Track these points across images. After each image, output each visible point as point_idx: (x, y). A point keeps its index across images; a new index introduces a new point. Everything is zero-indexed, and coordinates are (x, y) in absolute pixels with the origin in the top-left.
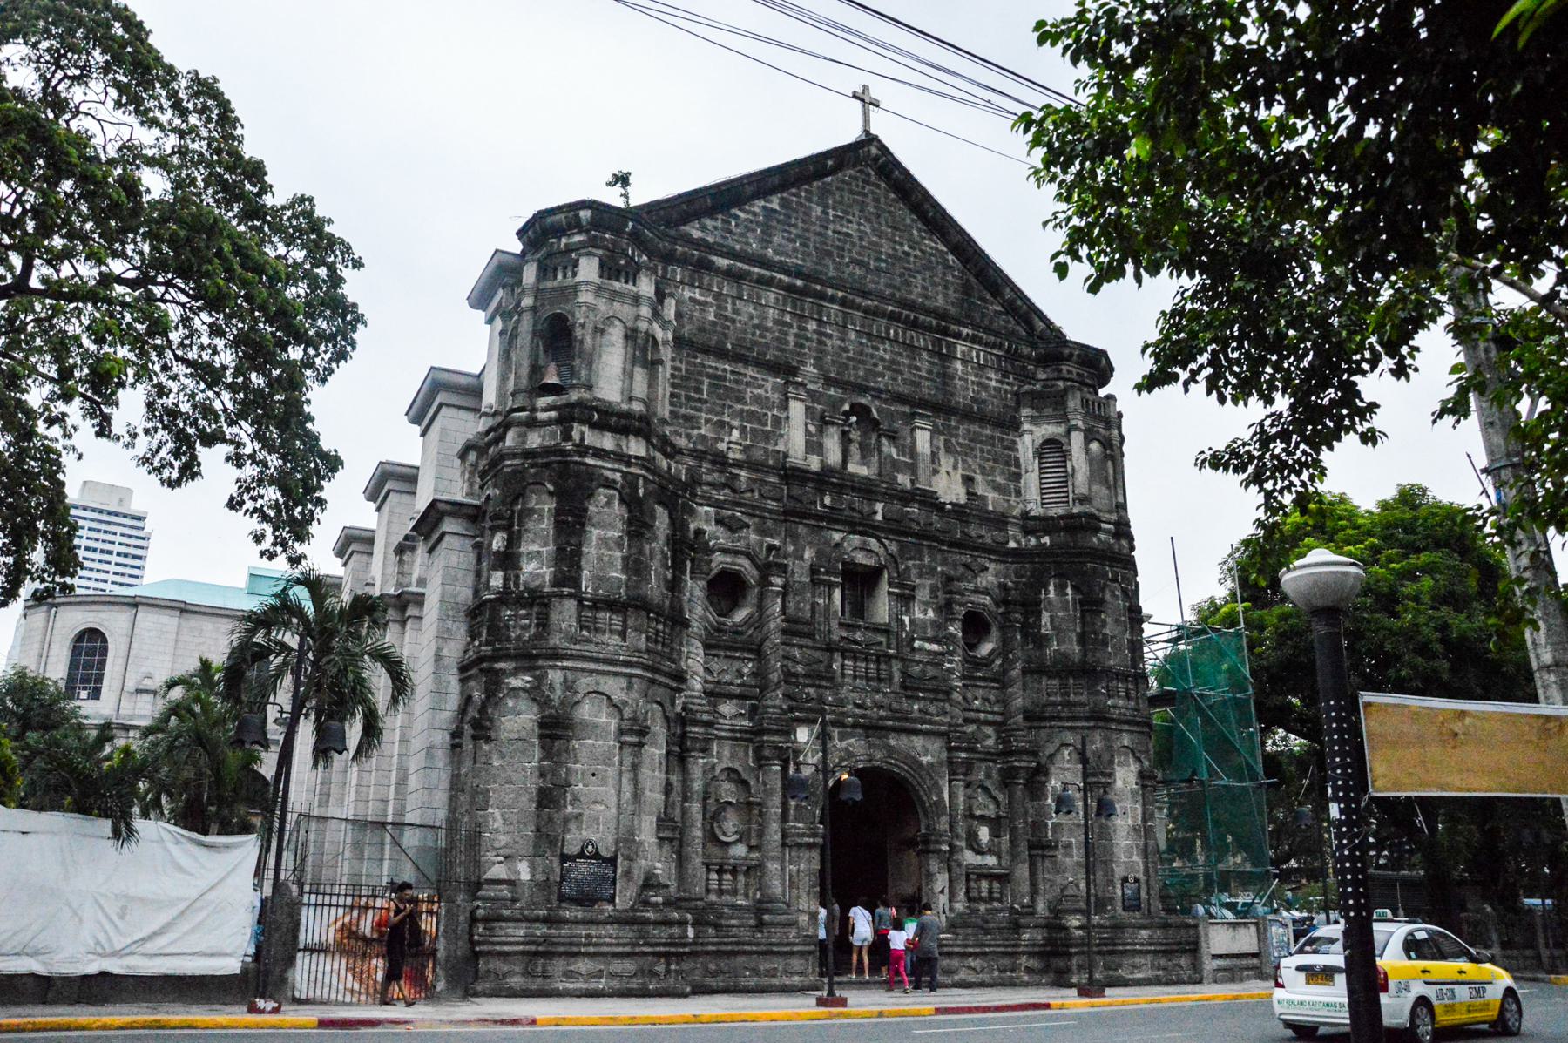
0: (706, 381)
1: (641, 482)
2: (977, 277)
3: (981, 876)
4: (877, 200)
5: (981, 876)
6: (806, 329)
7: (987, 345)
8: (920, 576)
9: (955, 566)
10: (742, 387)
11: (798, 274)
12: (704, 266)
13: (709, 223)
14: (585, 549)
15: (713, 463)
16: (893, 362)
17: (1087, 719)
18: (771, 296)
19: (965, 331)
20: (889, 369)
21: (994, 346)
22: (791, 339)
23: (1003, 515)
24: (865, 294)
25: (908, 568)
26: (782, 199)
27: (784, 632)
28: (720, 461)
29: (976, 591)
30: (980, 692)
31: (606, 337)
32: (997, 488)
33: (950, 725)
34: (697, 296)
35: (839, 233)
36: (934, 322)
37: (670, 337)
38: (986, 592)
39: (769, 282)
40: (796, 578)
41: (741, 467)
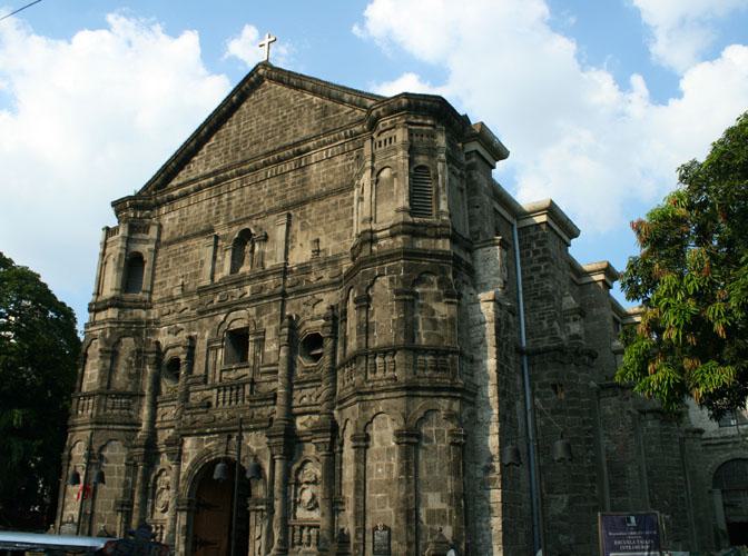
1: (108, 331)
7: (331, 143)
8: (270, 322)
12: (172, 200)
16: (269, 191)
18: (205, 194)
19: (310, 144)
20: (268, 196)
21: (335, 140)
23: (336, 256)
24: (244, 162)
30: (309, 391)
36: (290, 151)
37: (152, 246)
38: (319, 317)
39: (199, 189)
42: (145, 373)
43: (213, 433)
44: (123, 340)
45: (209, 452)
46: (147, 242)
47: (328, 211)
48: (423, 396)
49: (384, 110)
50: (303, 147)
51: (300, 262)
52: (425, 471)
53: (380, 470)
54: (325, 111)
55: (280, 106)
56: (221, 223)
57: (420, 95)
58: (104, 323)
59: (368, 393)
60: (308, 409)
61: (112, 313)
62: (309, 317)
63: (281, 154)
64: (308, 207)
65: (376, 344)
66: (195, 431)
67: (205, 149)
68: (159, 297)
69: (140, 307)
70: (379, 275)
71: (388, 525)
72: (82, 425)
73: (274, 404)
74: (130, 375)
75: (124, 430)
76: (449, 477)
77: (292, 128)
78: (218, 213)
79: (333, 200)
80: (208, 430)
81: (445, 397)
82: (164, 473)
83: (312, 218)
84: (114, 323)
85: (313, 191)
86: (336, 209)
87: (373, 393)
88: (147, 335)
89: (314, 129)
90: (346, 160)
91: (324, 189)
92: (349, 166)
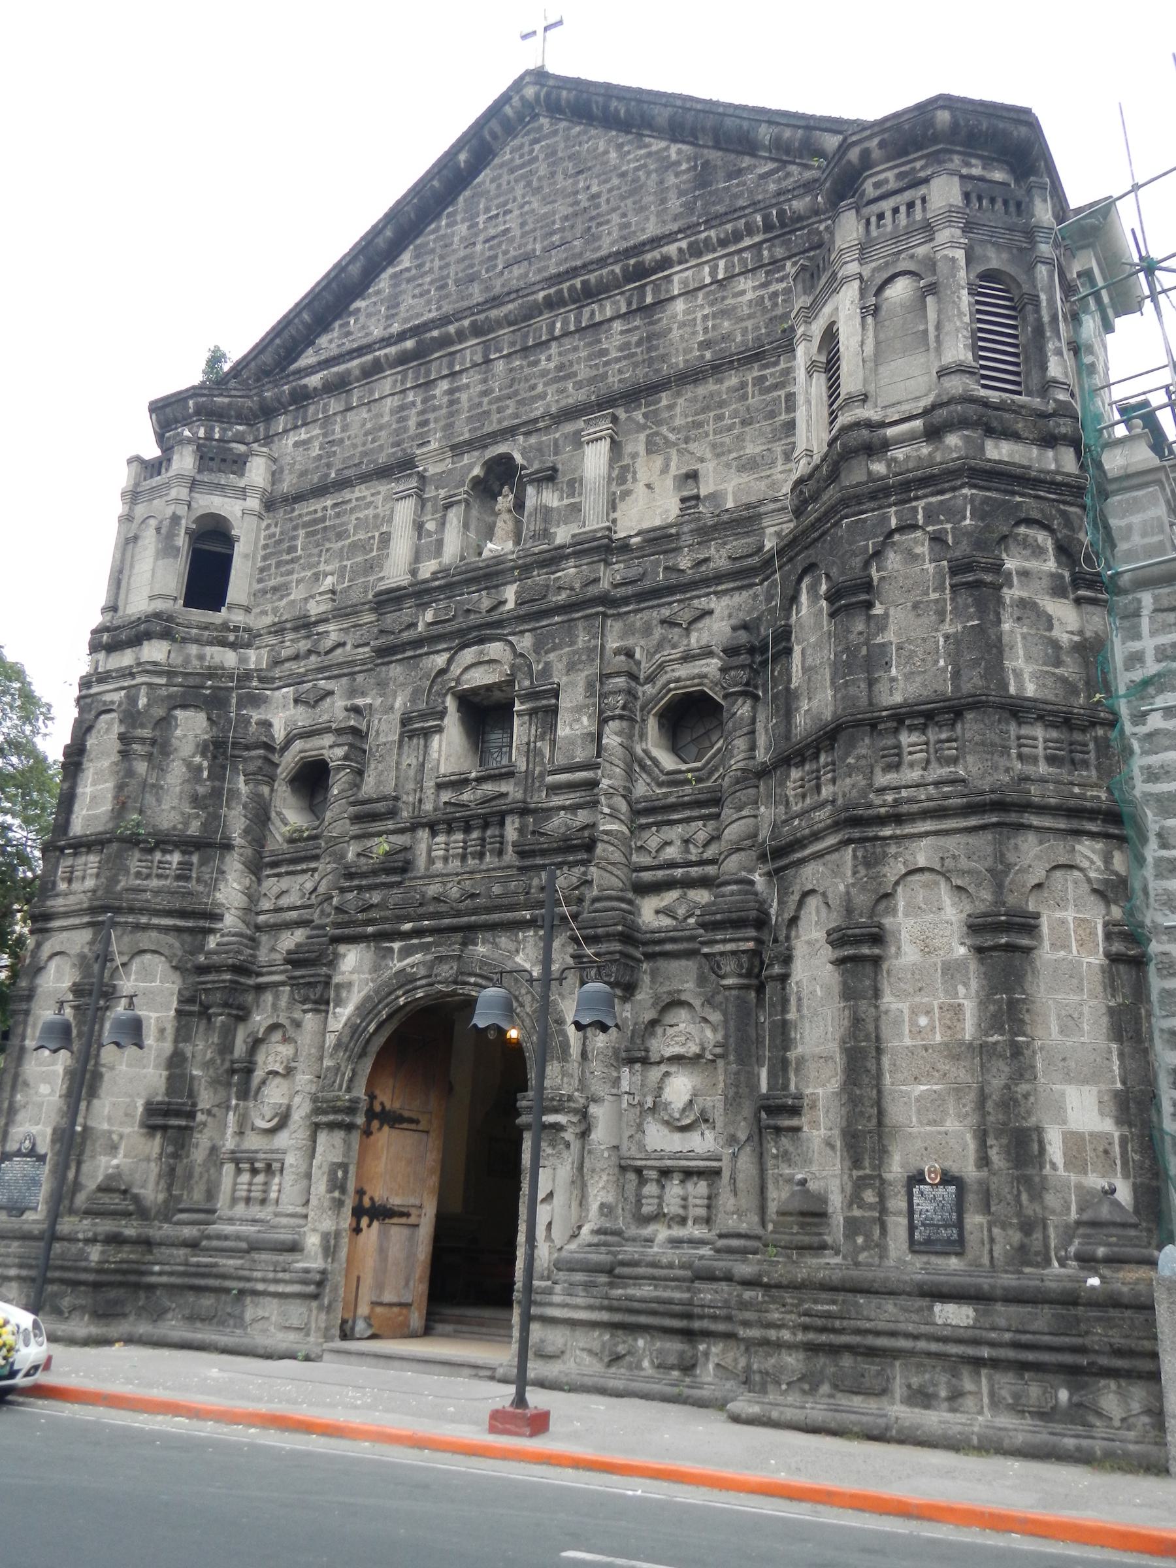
0: (301, 532)
1: (144, 690)
2: (717, 146)
3: (665, 1173)
4: (552, 153)
5: (665, 1173)
6: (434, 397)
7: (723, 243)
8: (571, 668)
9: (647, 631)
10: (345, 519)
11: (402, 336)
12: (302, 397)
13: (323, 341)
14: (79, 790)
15: (296, 629)
16: (560, 367)
17: (837, 826)
18: (386, 385)
19: (671, 249)
21: (737, 237)
22: (412, 423)
23: (749, 506)
25: (547, 664)
26: (416, 248)
27: (357, 819)
28: (304, 625)
29: (687, 658)
31: (140, 543)
32: (750, 465)
34: (304, 437)
35: (494, 237)
36: (617, 269)
37: (254, 503)
38: (707, 652)
40: (382, 739)
41: (326, 620)
42: (234, 794)
43: (418, 933)
44: (178, 713)
45: (405, 980)
46: (243, 493)
47: (721, 404)
48: (1038, 829)
49: (881, 145)
50: (649, 257)
51: (646, 525)
52: (1054, 1028)
53: (923, 1021)
54: (703, 177)
55: (580, 172)
56: (434, 445)
57: (982, 103)
58: (132, 675)
59: (882, 821)
60: (679, 872)
61: (155, 651)
62: (676, 653)
63: (592, 277)
64: (665, 399)
65: (898, 698)
66: (370, 929)
67: (384, 282)
68: (268, 620)
69: (223, 643)
70: (900, 529)
71: (955, 1169)
72: (66, 915)
73: (585, 863)
74: (195, 800)
75: (178, 930)
76: (1114, 1046)
77: (615, 218)
78: (423, 424)
79: (733, 380)
80: (408, 926)
81: (1092, 835)
82: (277, 1036)
83: (678, 422)
84: (159, 673)
85: (679, 361)
86: (744, 397)
87: (897, 819)
88: (240, 705)
89: (675, 218)
90: (764, 285)
91: (708, 355)
92: (775, 295)
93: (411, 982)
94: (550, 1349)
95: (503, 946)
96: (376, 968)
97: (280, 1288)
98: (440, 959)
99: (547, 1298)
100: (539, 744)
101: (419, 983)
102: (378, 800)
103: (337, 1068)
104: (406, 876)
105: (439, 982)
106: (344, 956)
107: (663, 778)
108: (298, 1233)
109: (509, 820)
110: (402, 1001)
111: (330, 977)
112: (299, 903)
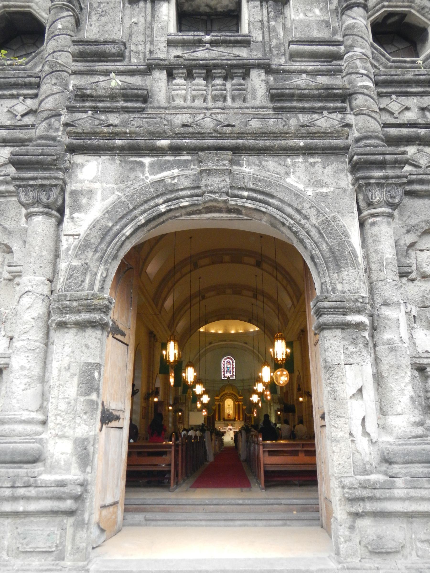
33: (358, 140)
66: (118, 142)
93: (172, 192)
94: (390, 545)
95: (271, 169)
96: (122, 179)
97: (20, 507)
98: (209, 172)
99: (387, 493)
100: (273, 23)
101: (181, 193)
102: (105, 42)
103: (86, 268)
104: (149, 105)
105: (214, 193)
106: (82, 166)
107: (390, 64)
108: (41, 441)
109: (254, 73)
110: (163, 208)
111: (65, 184)
112: (8, 123)
